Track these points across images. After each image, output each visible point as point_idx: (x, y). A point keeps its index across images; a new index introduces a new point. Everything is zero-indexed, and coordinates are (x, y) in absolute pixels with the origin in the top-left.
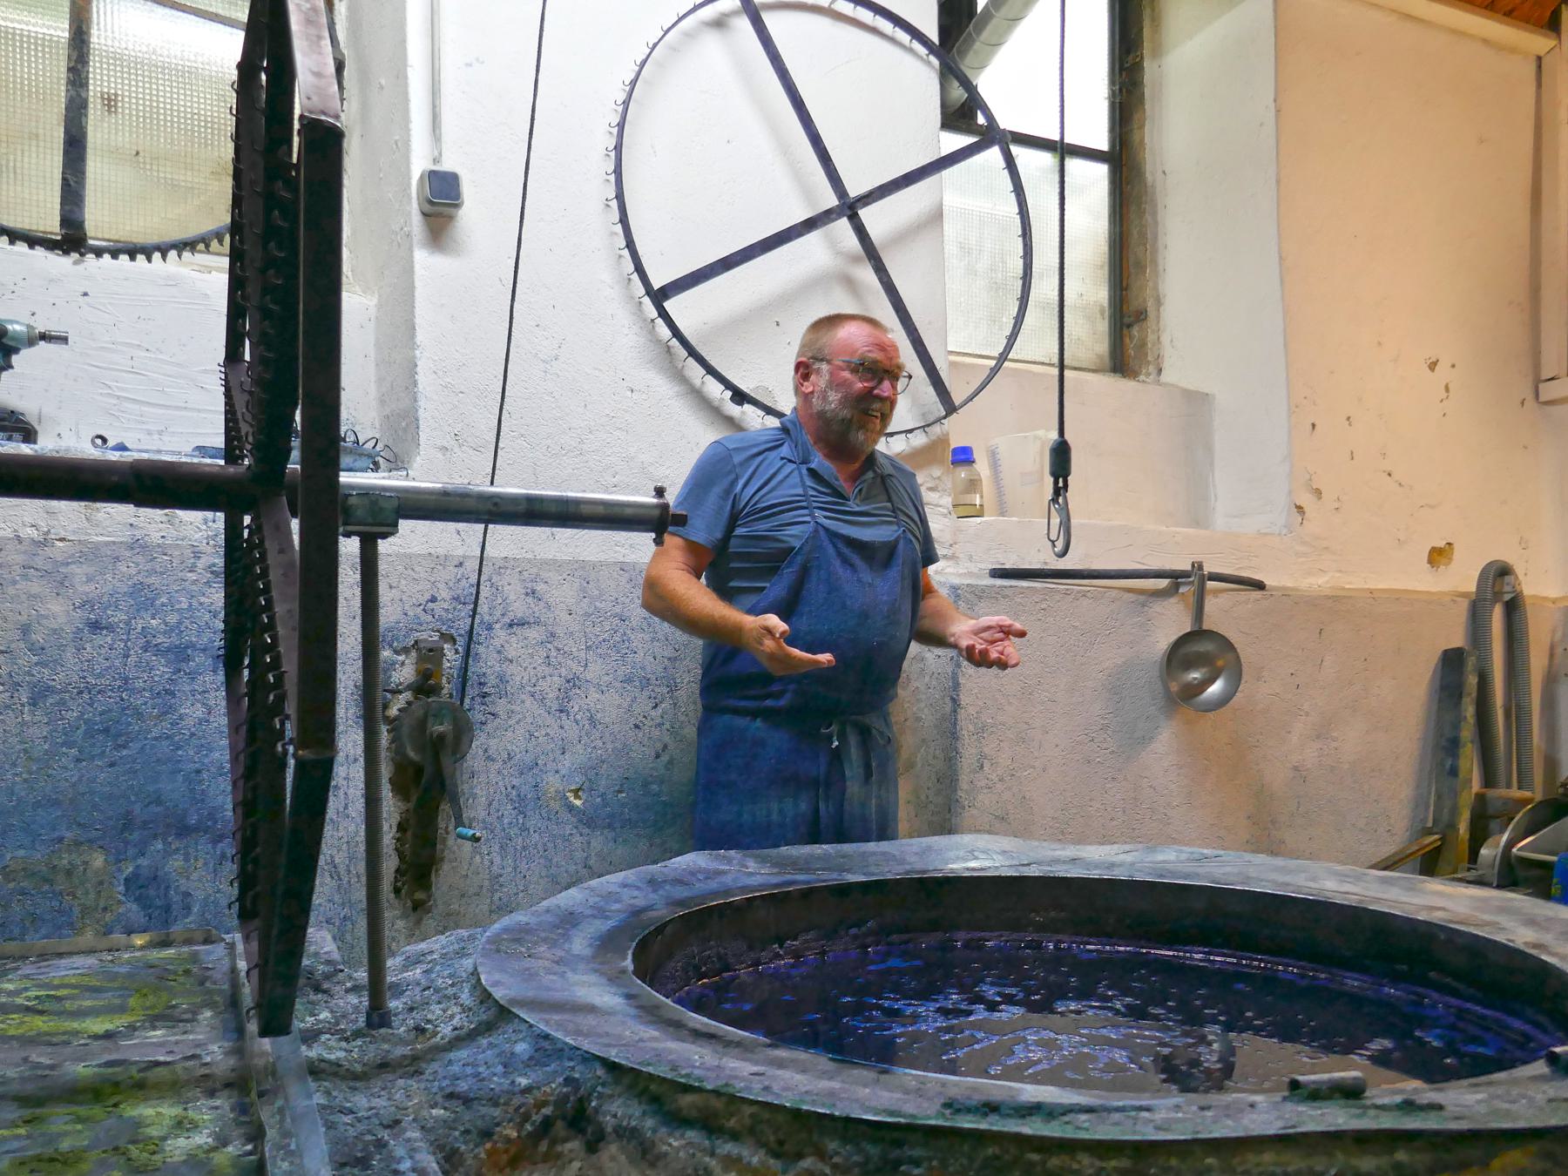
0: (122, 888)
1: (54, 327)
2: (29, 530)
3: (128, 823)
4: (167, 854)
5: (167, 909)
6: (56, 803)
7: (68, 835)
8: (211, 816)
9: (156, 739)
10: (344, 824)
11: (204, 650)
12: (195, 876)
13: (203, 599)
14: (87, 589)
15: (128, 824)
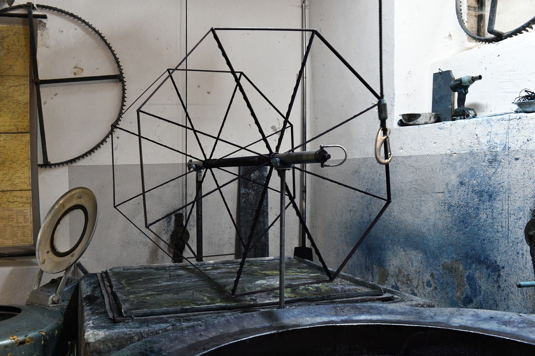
0: (465, 279)
1: (476, 75)
2: (449, 151)
3: (467, 256)
4: (476, 270)
5: (476, 290)
6: (452, 245)
7: (455, 256)
8: (487, 258)
9: (474, 226)
10: (525, 271)
11: (487, 192)
12: (482, 280)
13: (487, 173)
14: (460, 170)
15: (467, 256)
